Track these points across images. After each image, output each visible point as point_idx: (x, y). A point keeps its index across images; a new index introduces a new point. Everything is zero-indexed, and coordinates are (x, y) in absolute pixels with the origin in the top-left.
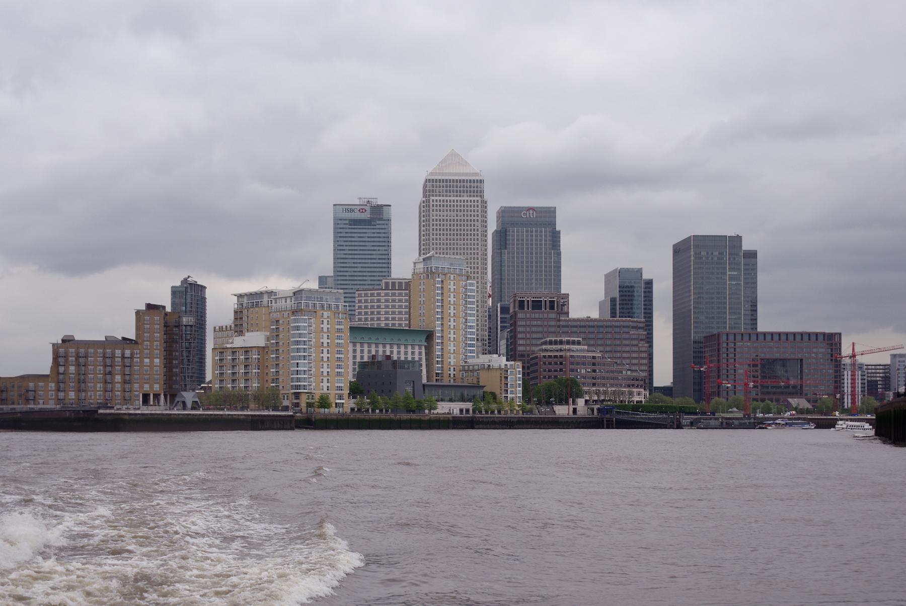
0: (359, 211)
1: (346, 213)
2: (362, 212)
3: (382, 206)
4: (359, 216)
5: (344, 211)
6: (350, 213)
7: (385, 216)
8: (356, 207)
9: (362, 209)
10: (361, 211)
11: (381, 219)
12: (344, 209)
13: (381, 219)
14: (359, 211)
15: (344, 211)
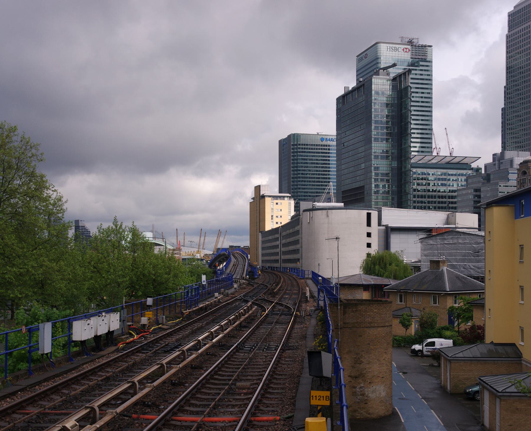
0: (403, 50)
1: (391, 52)
2: (406, 52)
3: (425, 46)
4: (403, 56)
5: (389, 50)
6: (394, 52)
7: (428, 58)
8: (400, 46)
9: (406, 49)
10: (405, 50)
11: (425, 60)
12: (389, 48)
13: (425, 60)
14: (403, 50)
15: (389, 50)
